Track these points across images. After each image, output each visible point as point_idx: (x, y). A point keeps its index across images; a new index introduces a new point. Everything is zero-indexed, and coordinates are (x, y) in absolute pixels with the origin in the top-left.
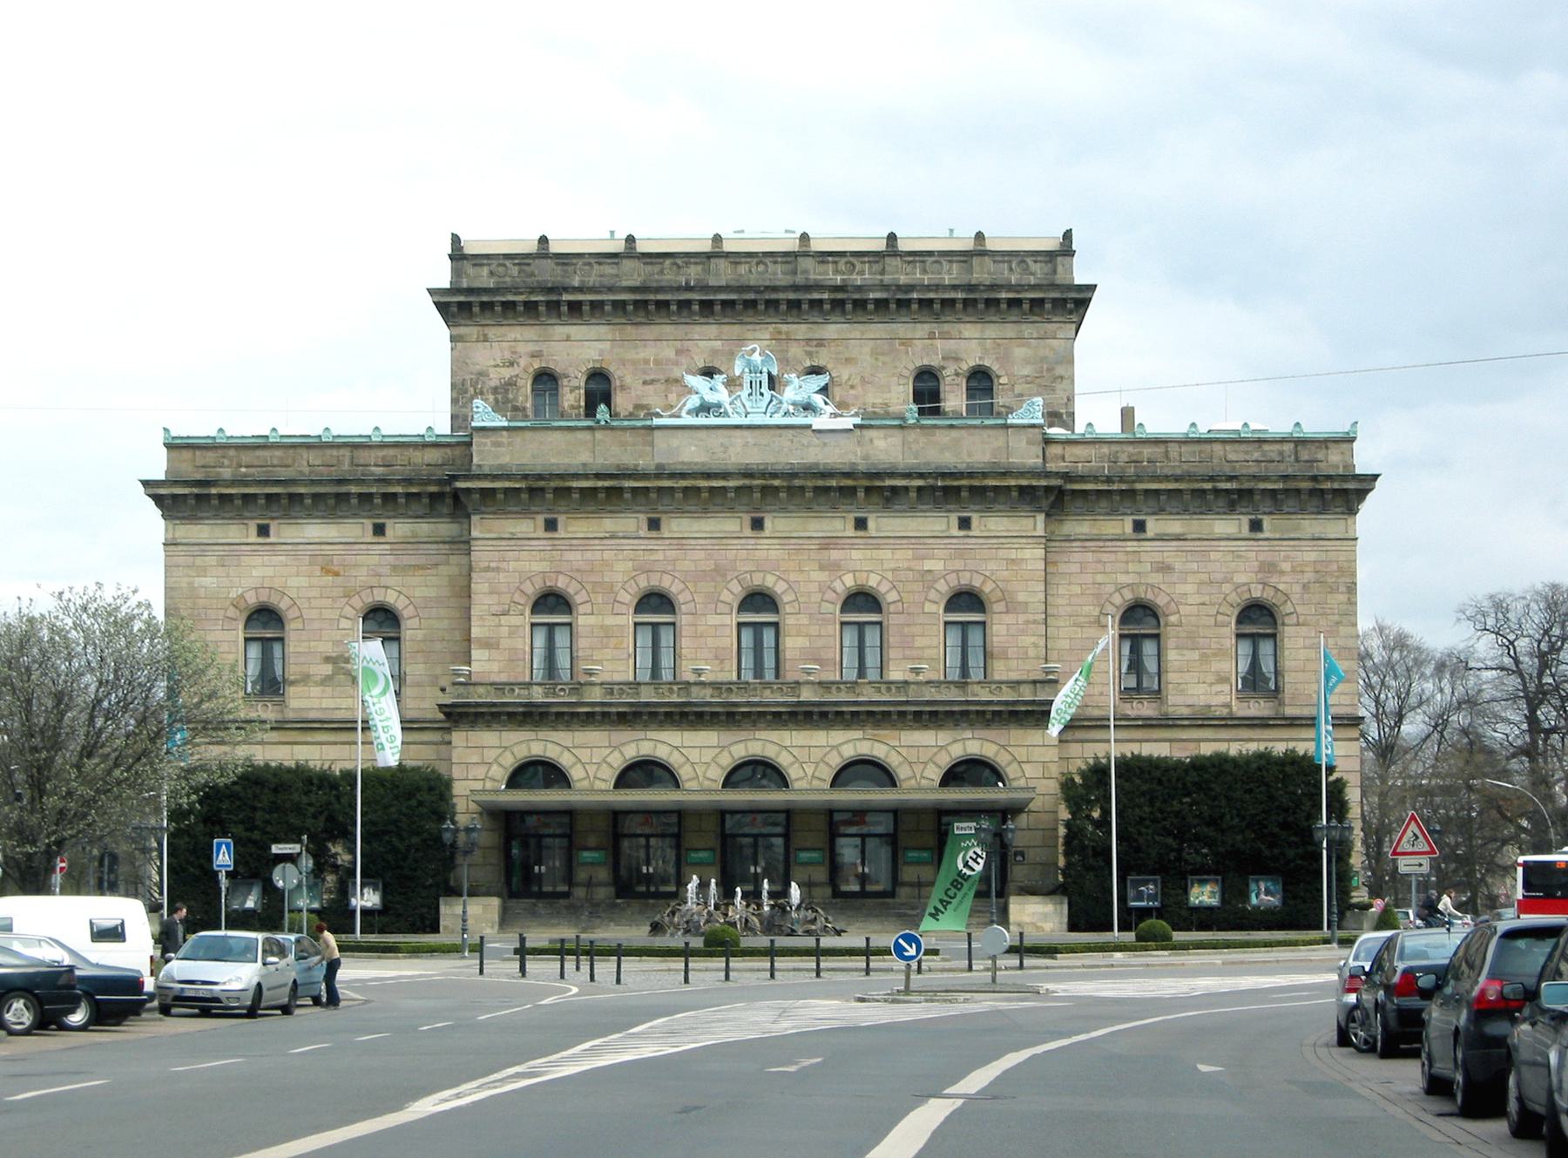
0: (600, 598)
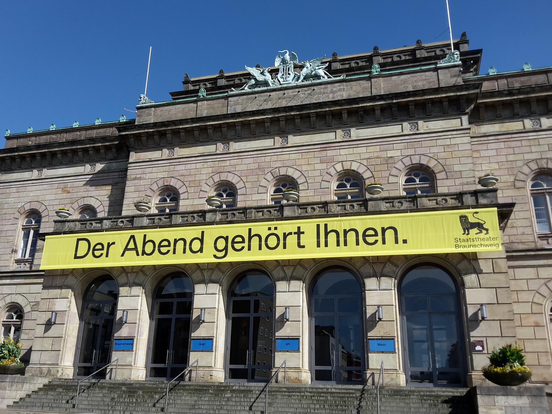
0: (192, 190)
